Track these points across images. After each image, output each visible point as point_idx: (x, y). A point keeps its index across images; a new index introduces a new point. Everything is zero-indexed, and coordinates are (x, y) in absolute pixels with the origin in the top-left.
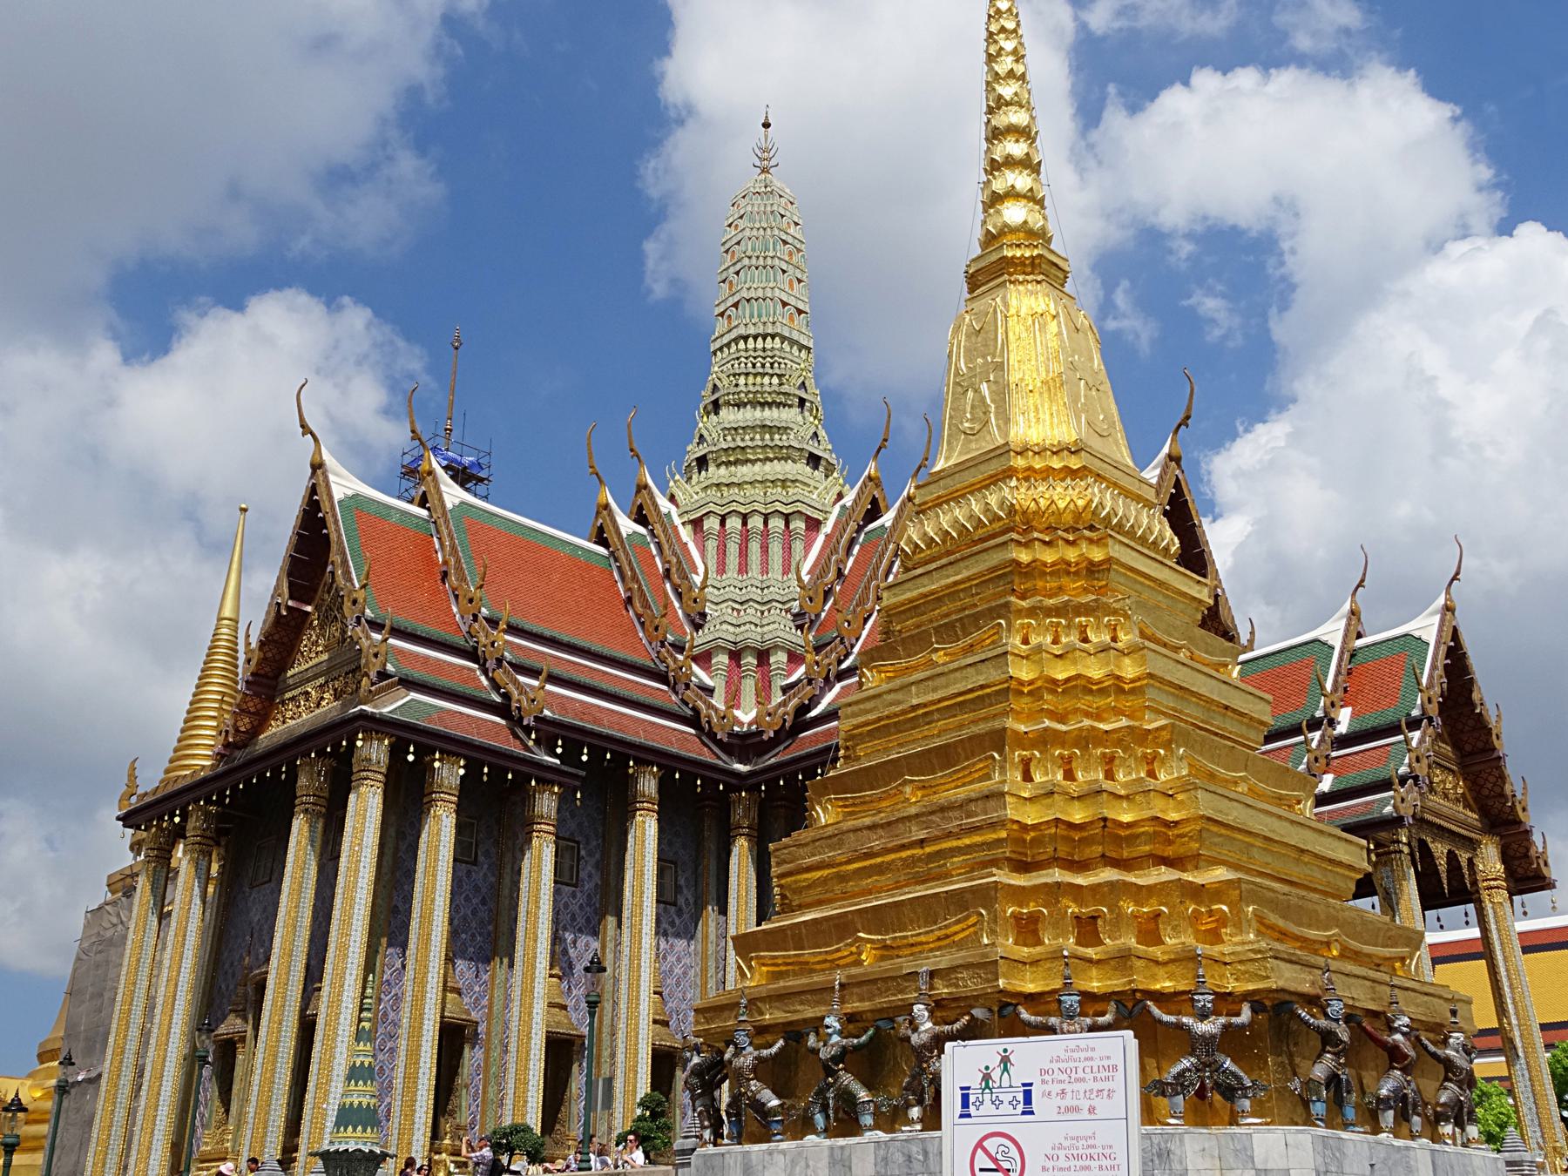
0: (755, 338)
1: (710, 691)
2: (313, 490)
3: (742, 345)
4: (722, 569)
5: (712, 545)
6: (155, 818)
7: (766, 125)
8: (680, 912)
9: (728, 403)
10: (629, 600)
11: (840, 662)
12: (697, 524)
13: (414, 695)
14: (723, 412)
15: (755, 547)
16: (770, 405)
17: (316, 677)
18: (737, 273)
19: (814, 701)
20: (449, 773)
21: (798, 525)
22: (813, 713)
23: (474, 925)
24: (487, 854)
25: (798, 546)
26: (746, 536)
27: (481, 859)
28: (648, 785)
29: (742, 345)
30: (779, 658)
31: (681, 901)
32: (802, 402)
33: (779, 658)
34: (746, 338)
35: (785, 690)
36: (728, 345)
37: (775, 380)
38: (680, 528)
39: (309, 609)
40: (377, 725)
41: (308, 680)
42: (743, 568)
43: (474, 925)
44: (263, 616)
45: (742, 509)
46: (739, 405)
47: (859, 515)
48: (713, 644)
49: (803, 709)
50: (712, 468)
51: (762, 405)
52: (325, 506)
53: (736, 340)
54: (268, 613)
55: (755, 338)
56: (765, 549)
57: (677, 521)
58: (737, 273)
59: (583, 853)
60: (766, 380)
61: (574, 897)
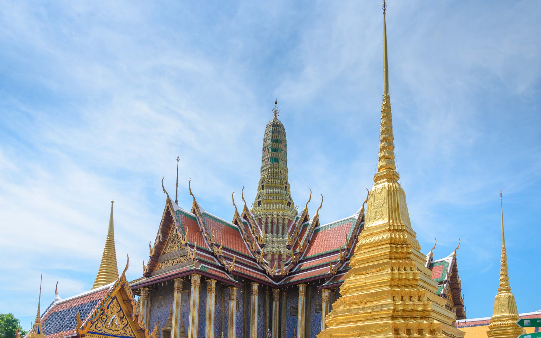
5: (263, 226)
8: (260, 316)
13: (202, 264)
15: (275, 227)
19: (294, 268)
20: (213, 284)
22: (293, 271)
25: (286, 227)
26: (272, 223)
28: (256, 287)
30: (284, 257)
32: (286, 187)
49: (291, 270)
56: (278, 227)
60: (277, 181)
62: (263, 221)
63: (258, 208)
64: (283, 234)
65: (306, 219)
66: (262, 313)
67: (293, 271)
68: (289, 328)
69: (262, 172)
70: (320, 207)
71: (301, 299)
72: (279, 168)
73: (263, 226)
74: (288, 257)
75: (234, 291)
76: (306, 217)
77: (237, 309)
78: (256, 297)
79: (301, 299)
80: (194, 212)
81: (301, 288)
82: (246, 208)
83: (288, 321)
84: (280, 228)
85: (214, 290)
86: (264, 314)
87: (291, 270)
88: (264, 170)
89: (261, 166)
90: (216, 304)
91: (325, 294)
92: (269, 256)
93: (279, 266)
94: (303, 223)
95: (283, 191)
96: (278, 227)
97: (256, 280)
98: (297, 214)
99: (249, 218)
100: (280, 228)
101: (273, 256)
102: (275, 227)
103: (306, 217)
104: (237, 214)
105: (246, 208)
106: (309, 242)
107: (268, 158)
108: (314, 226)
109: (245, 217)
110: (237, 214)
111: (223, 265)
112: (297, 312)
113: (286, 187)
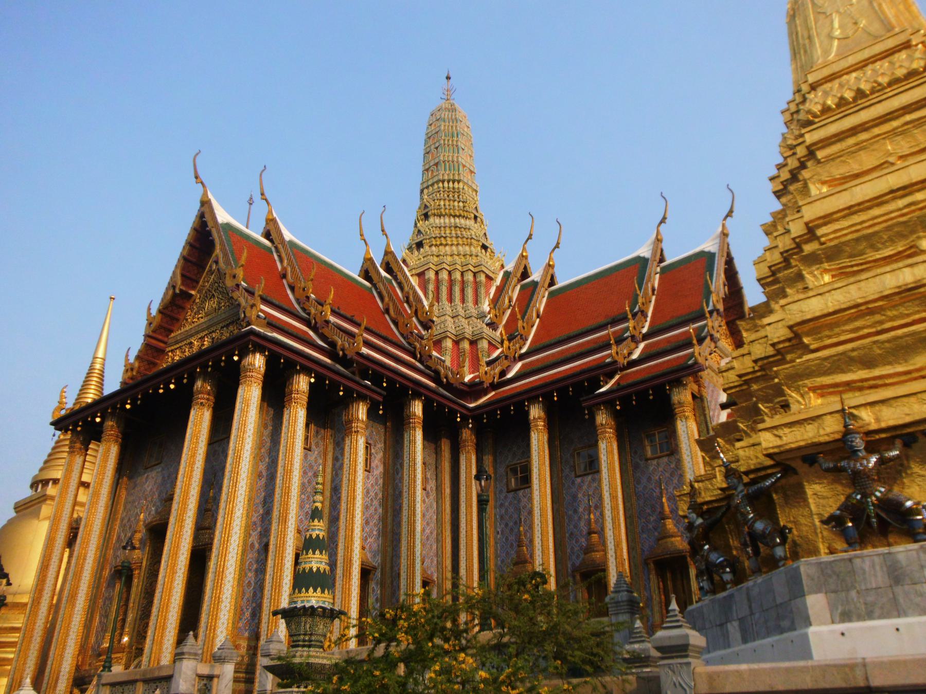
0: (448, 182)
1: (444, 361)
2: (202, 216)
3: (441, 185)
4: (438, 298)
5: (431, 287)
6: (80, 425)
7: (448, 78)
8: (428, 495)
9: (434, 215)
10: (387, 311)
11: (521, 348)
12: (421, 275)
14: (431, 220)
15: (457, 289)
16: (459, 216)
17: (198, 332)
18: (437, 148)
19: (509, 368)
20: (302, 383)
21: (482, 278)
22: (509, 376)
23: (309, 490)
24: (317, 445)
26: (451, 283)
27: (313, 447)
28: (417, 408)
29: (441, 185)
30: (484, 344)
31: (428, 488)
32: (476, 217)
33: (484, 344)
34: (443, 182)
35: (489, 363)
36: (432, 185)
37: (461, 204)
38: (410, 278)
39: (193, 292)
40: (260, 344)
41: (192, 336)
42: (451, 299)
43: (309, 490)
44: (161, 296)
45: (448, 268)
46: (440, 216)
47: (519, 275)
48: (443, 335)
50: (427, 247)
51: (454, 216)
52: (210, 224)
53: (437, 182)
54: (165, 294)
55: (448, 182)
57: (408, 274)
58: (437, 148)
59: (373, 451)
61: (368, 478)
62: (431, 275)
63: (416, 253)
64: (476, 302)
65: (525, 274)
66: (432, 485)
67: (509, 376)
68: (507, 525)
69: (422, 191)
70: (557, 246)
71: (538, 440)
72: (459, 182)
73: (431, 287)
74: (492, 346)
75: (361, 411)
76: (525, 268)
77: (368, 470)
78: (419, 435)
79: (538, 440)
80: (267, 235)
81: (535, 412)
82: (388, 253)
83: (502, 505)
84: (470, 292)
85: (304, 399)
86: (439, 489)
87: (503, 373)
88: (427, 187)
89: (420, 181)
90: (307, 449)
91: (602, 418)
92: (449, 344)
93: (475, 366)
94: (519, 281)
95: (470, 223)
96: (463, 291)
97: (418, 391)
98: (502, 266)
99: (395, 269)
100: (470, 292)
101: (456, 343)
102: (457, 289)
103: (525, 268)
104: (369, 261)
105: (388, 253)
106: (538, 316)
107: (436, 164)
108: (546, 285)
109: (388, 269)
110: (369, 261)
111: (333, 344)
112: (526, 481)
113: (476, 217)
